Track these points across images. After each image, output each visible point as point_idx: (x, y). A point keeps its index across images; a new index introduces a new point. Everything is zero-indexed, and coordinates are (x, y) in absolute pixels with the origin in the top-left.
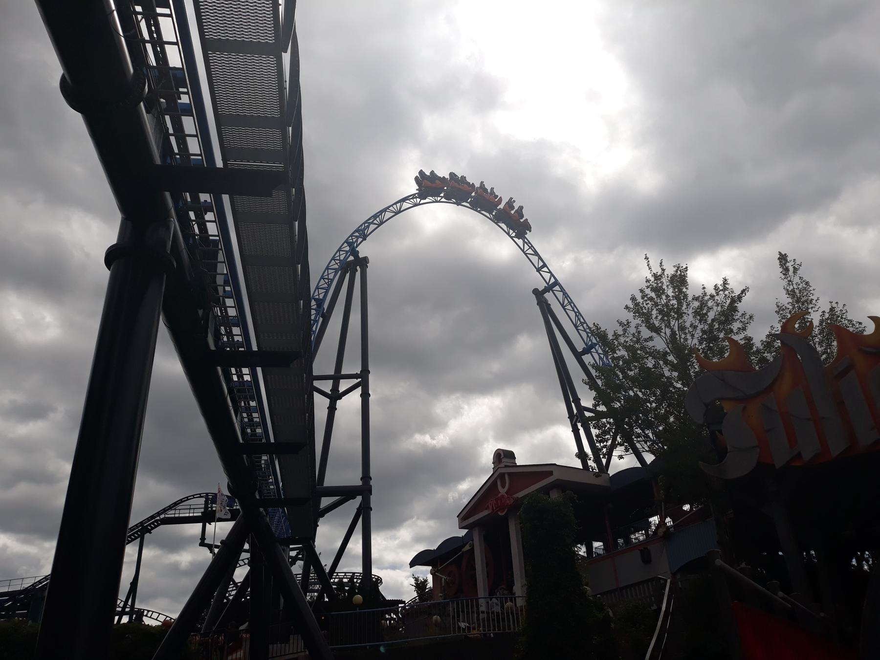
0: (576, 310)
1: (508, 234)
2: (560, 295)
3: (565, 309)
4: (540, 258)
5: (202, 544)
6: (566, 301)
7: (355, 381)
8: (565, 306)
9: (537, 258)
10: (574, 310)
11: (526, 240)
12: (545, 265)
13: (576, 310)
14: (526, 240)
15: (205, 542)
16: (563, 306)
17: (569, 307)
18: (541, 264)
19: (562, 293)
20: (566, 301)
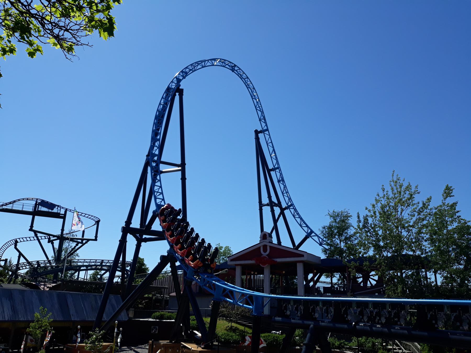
0: (289, 197)
1: (256, 107)
2: (278, 174)
3: (283, 195)
4: (266, 125)
5: (31, 230)
6: (285, 192)
7: (156, 196)
8: (284, 194)
9: (265, 124)
10: (288, 197)
11: (263, 114)
12: (267, 130)
13: (289, 197)
14: (263, 114)
15: (33, 229)
16: (282, 193)
17: (286, 195)
18: (265, 128)
19: (300, 219)
20: (285, 192)
